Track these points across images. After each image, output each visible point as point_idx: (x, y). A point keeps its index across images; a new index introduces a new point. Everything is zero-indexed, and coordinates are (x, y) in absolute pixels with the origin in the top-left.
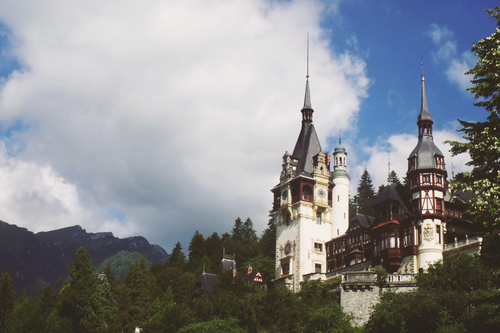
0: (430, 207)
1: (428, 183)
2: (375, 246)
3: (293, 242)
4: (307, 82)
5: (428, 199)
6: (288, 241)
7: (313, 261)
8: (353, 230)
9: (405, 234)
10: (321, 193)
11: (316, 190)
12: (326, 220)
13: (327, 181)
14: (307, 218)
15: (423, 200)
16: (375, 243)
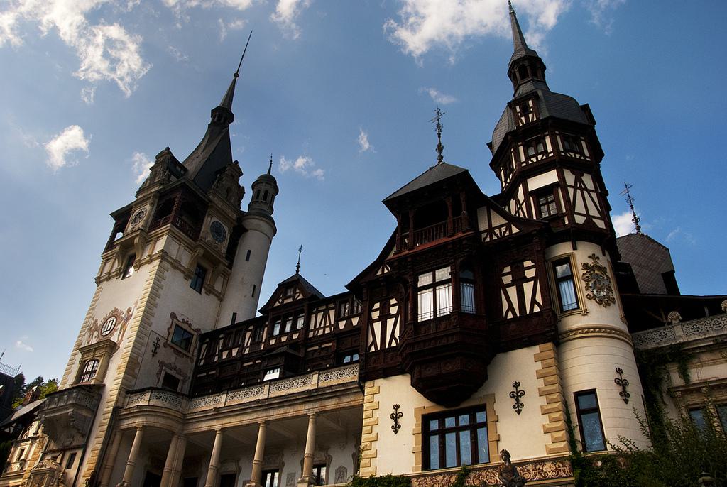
0: (594, 212)
1: (578, 156)
2: (376, 321)
3: (125, 312)
4: (235, 80)
5: (585, 192)
6: (116, 310)
7: (162, 364)
8: (282, 305)
9: (507, 280)
10: (217, 231)
11: (209, 221)
12: (213, 287)
13: (235, 217)
14: (175, 267)
15: (571, 191)
16: (375, 315)
